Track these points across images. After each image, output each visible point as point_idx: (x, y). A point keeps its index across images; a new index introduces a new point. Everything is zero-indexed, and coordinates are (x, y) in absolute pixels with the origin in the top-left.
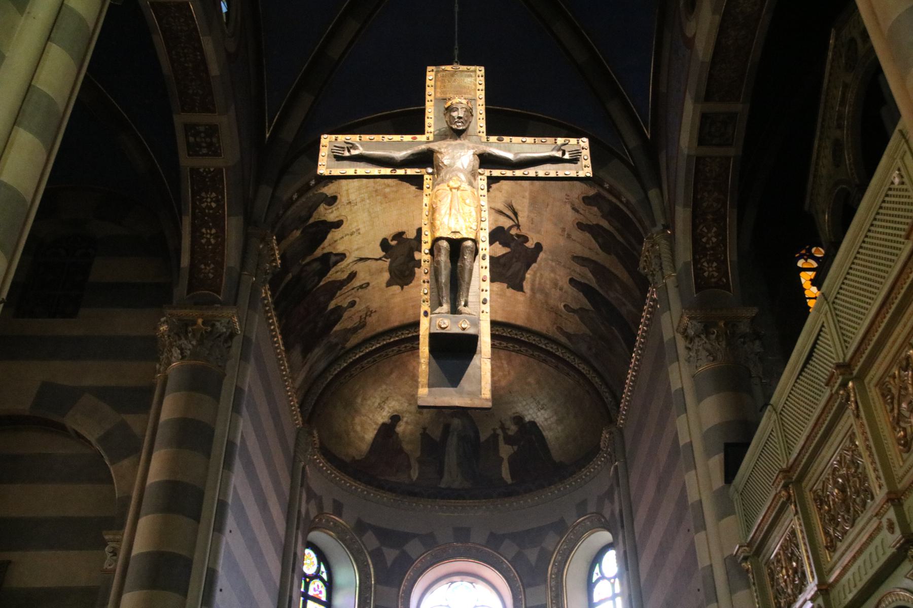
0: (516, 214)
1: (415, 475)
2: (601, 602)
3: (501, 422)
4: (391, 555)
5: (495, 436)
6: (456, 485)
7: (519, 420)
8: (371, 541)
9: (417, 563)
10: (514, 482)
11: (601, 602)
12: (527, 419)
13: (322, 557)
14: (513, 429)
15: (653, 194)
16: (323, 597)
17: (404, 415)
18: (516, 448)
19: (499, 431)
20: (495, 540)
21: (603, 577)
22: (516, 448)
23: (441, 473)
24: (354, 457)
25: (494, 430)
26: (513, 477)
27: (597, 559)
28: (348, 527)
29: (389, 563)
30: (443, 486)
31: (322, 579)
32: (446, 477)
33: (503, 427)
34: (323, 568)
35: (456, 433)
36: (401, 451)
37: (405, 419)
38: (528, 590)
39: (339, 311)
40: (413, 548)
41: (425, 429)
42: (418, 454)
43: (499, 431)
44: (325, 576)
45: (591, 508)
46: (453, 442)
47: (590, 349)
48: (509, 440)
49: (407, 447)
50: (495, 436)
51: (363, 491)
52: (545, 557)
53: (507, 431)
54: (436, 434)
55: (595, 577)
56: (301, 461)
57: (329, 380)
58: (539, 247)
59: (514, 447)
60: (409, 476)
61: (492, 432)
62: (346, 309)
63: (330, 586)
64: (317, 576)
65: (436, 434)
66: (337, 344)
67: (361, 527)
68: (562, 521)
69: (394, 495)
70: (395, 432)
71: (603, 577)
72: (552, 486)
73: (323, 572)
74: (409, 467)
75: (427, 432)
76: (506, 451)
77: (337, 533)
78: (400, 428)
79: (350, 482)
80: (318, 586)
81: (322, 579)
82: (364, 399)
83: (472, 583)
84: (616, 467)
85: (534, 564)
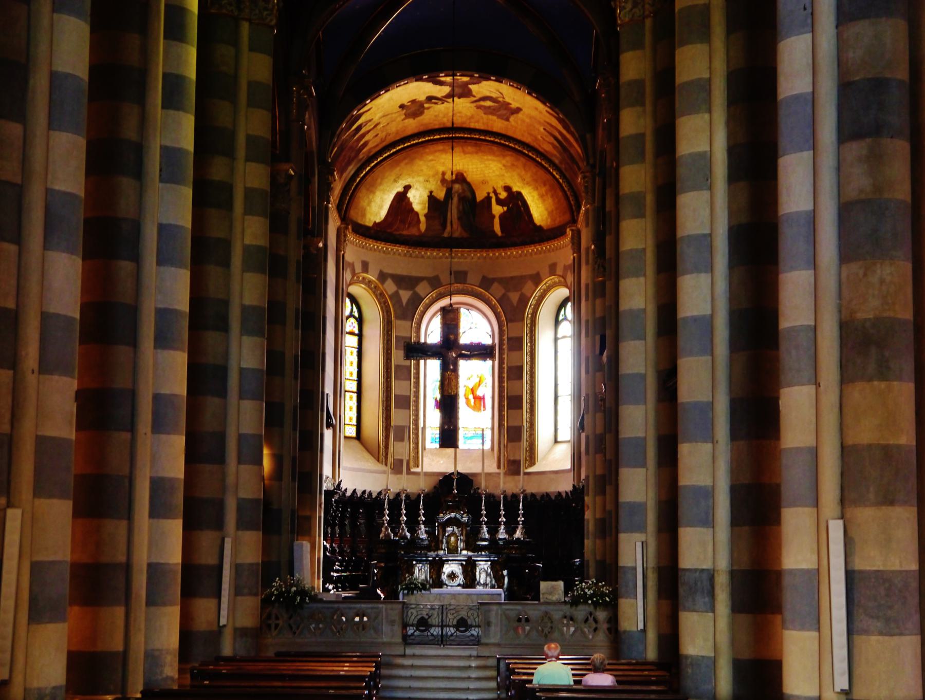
0: (502, 94)
1: (423, 227)
2: (564, 337)
3: (494, 188)
4: (405, 295)
5: (488, 198)
6: (456, 234)
7: (507, 189)
8: (390, 287)
9: (426, 301)
10: (504, 235)
11: (564, 337)
12: (515, 189)
13: (354, 300)
14: (503, 195)
15: (588, 136)
16: (357, 331)
17: (414, 184)
18: (505, 208)
19: (492, 195)
20: (486, 283)
21: (565, 319)
22: (505, 208)
23: (444, 226)
24: (375, 222)
25: (488, 194)
26: (502, 231)
27: (563, 305)
28: (374, 279)
29: (404, 304)
30: (446, 235)
31: (354, 317)
32: (449, 228)
33: (495, 192)
34: (355, 309)
35: (456, 195)
36: (412, 210)
37: (415, 187)
38: (510, 325)
39: (366, 144)
40: (421, 289)
41: (431, 192)
42: (426, 211)
43: (492, 195)
44: (356, 314)
45: (559, 271)
46: (455, 200)
47: (561, 163)
48: (500, 202)
49: (417, 207)
50: (488, 198)
51: (382, 248)
52: (524, 301)
53: (499, 195)
54: (441, 194)
55: (561, 318)
56: (341, 251)
57: (357, 181)
58: (518, 110)
59: (504, 208)
60: (419, 229)
61: (486, 195)
62: (372, 139)
63: (360, 321)
64: (351, 315)
65: (441, 194)
66: (363, 157)
67: (383, 277)
68: (538, 274)
69: (407, 247)
70: (406, 197)
71: (565, 319)
72: (533, 246)
73: (354, 312)
74: (419, 221)
75: (433, 194)
76: (497, 210)
77: (365, 284)
78: (410, 195)
79: (372, 244)
80: (352, 323)
81: (354, 317)
82: (382, 179)
83: (468, 310)
84: (574, 258)
85: (515, 304)
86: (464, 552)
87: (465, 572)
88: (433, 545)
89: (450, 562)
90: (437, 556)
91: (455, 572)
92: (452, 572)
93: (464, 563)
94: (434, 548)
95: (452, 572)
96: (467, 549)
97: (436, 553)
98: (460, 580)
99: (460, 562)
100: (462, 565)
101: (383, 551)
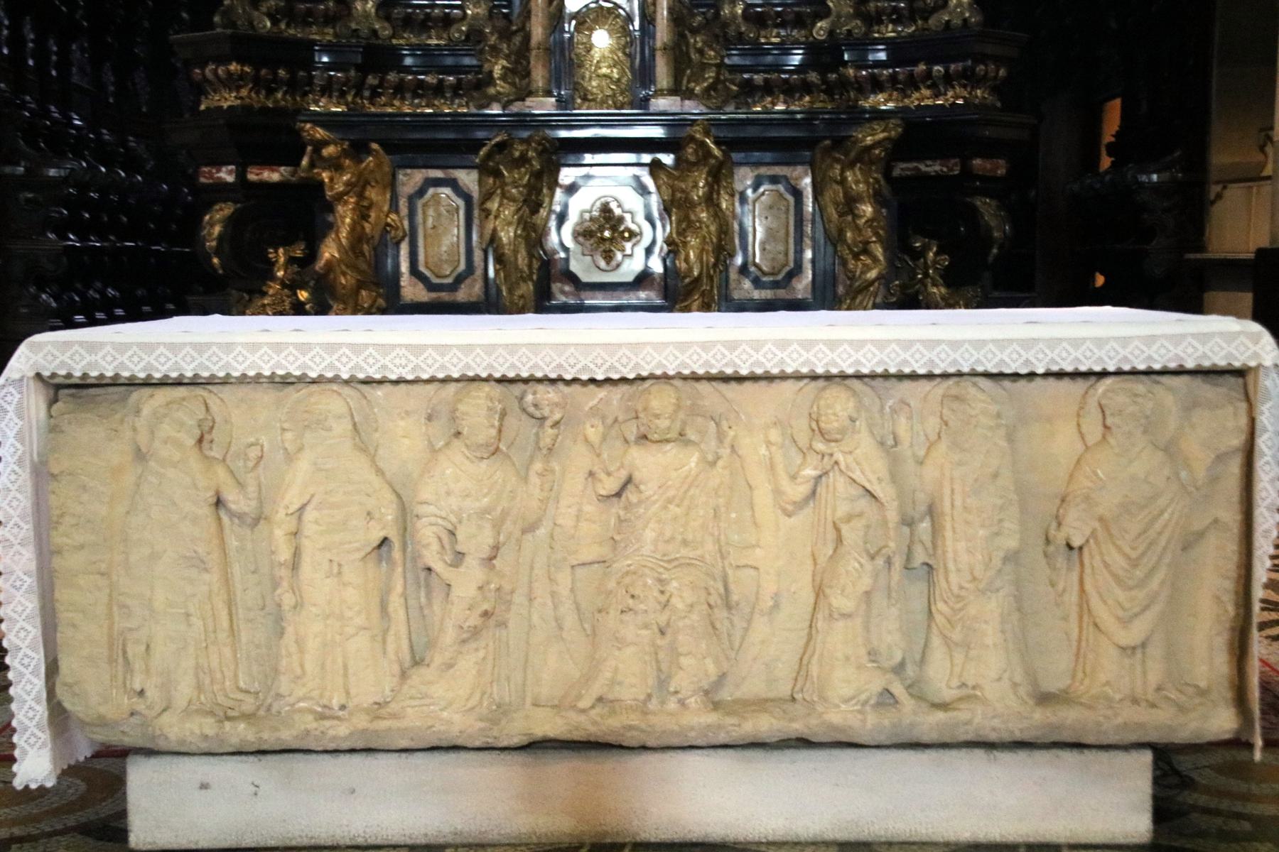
86: (662, 104)
87: (676, 205)
88: (497, 71)
89: (588, 158)
90: (524, 121)
91: (617, 212)
92: (606, 209)
93: (667, 159)
94: (501, 87)
95: (606, 209)
96: (674, 91)
97: (516, 108)
98: (649, 251)
99: (646, 158)
100: (655, 167)
101: (228, 100)
